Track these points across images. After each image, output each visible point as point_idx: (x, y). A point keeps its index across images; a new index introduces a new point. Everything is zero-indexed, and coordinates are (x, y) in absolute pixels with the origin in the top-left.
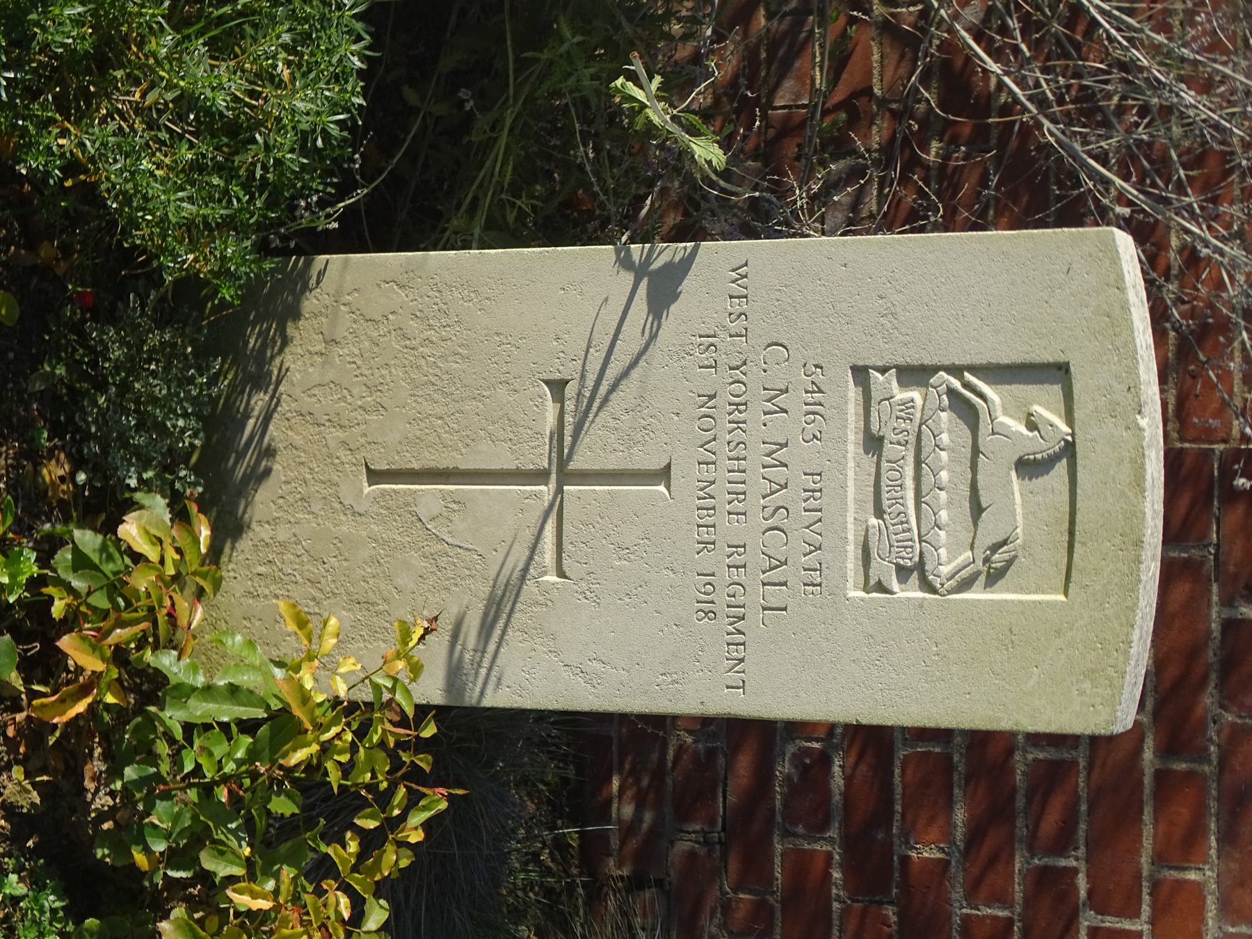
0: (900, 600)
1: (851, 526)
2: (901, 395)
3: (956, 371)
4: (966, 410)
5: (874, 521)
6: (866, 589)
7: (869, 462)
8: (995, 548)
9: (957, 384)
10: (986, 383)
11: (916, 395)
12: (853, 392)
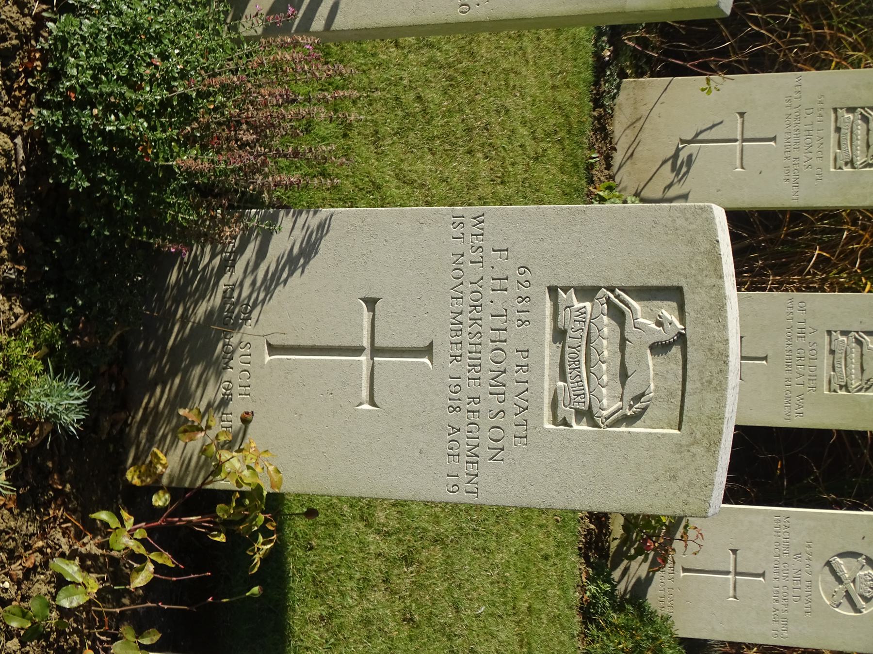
0: (840, 395)
1: (825, 375)
2: (841, 338)
3: (857, 332)
4: (859, 343)
5: (832, 373)
6: (830, 391)
7: (832, 356)
8: (868, 380)
9: (857, 336)
10: (867, 336)
11: (845, 339)
12: (827, 338)
